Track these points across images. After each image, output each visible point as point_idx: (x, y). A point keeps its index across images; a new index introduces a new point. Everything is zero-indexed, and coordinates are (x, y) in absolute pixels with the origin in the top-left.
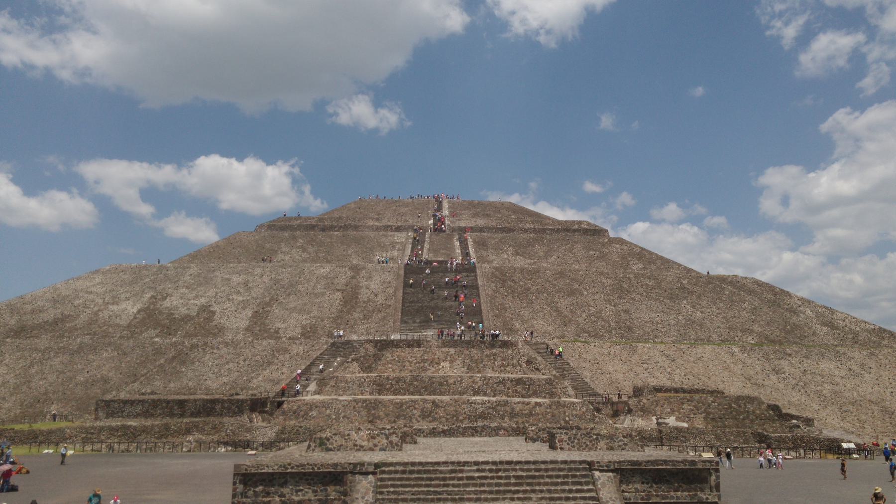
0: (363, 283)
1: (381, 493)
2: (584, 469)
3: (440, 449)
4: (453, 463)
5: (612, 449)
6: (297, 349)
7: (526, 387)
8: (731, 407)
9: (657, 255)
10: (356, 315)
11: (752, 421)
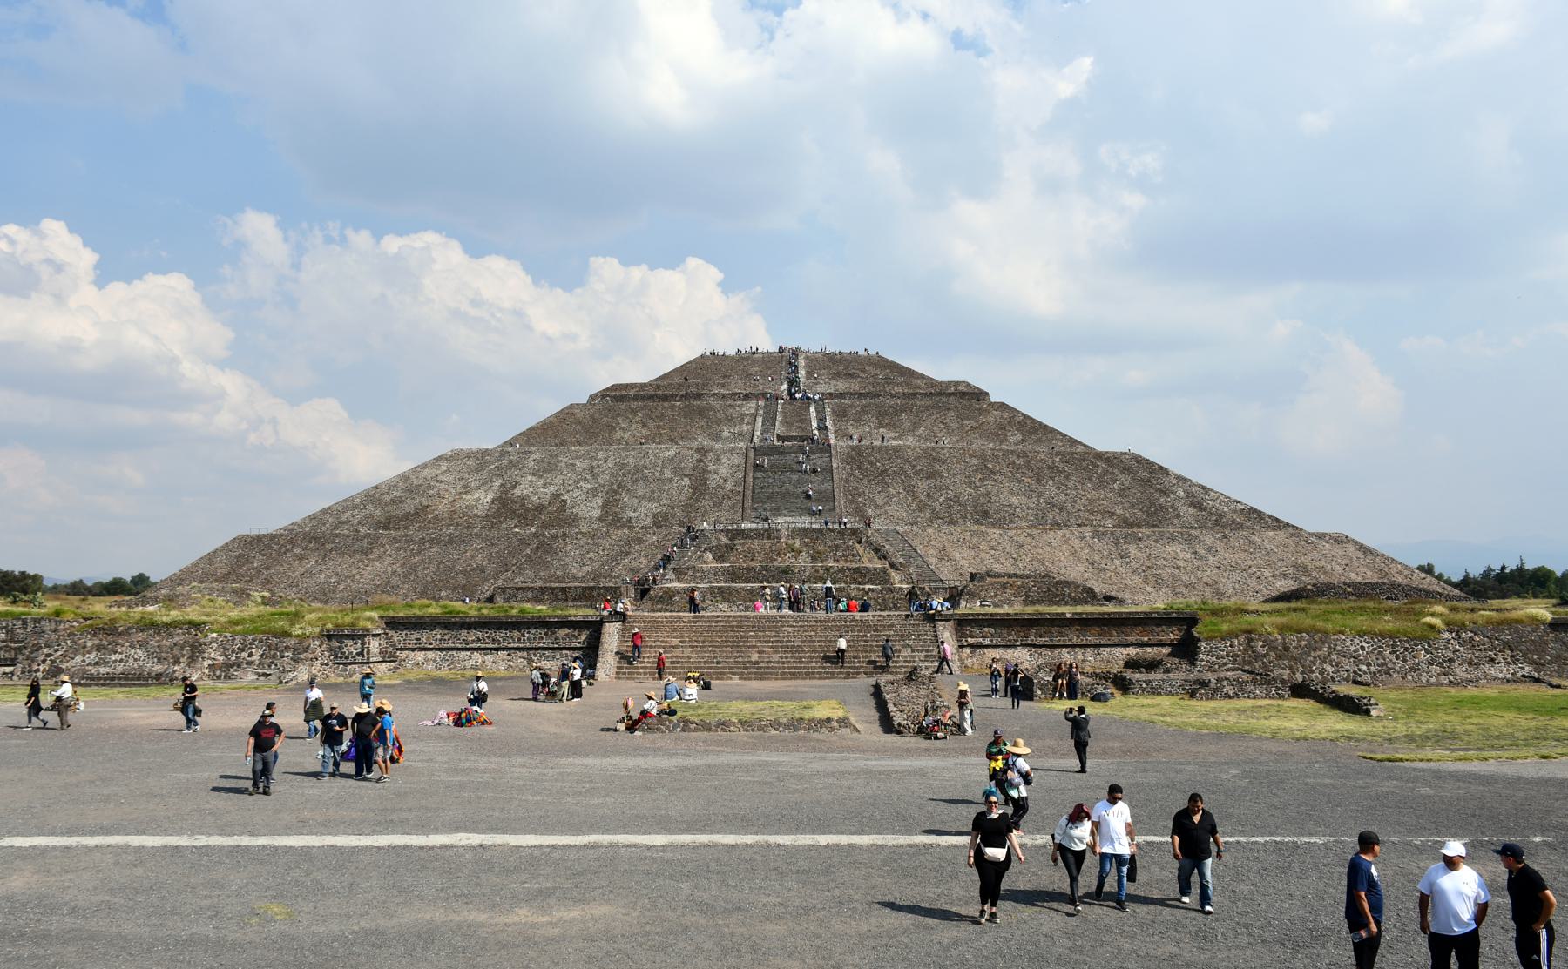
0: (711, 467)
10: (705, 502)
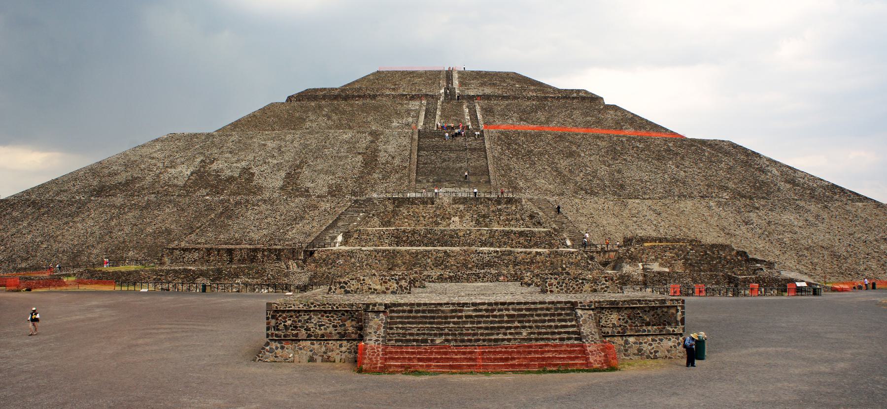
0: (382, 147)
1: (391, 329)
2: (568, 308)
3: (444, 293)
4: (453, 304)
5: (595, 291)
6: (325, 205)
7: (529, 239)
8: (706, 254)
9: (647, 121)
10: (376, 176)
11: (723, 265)
